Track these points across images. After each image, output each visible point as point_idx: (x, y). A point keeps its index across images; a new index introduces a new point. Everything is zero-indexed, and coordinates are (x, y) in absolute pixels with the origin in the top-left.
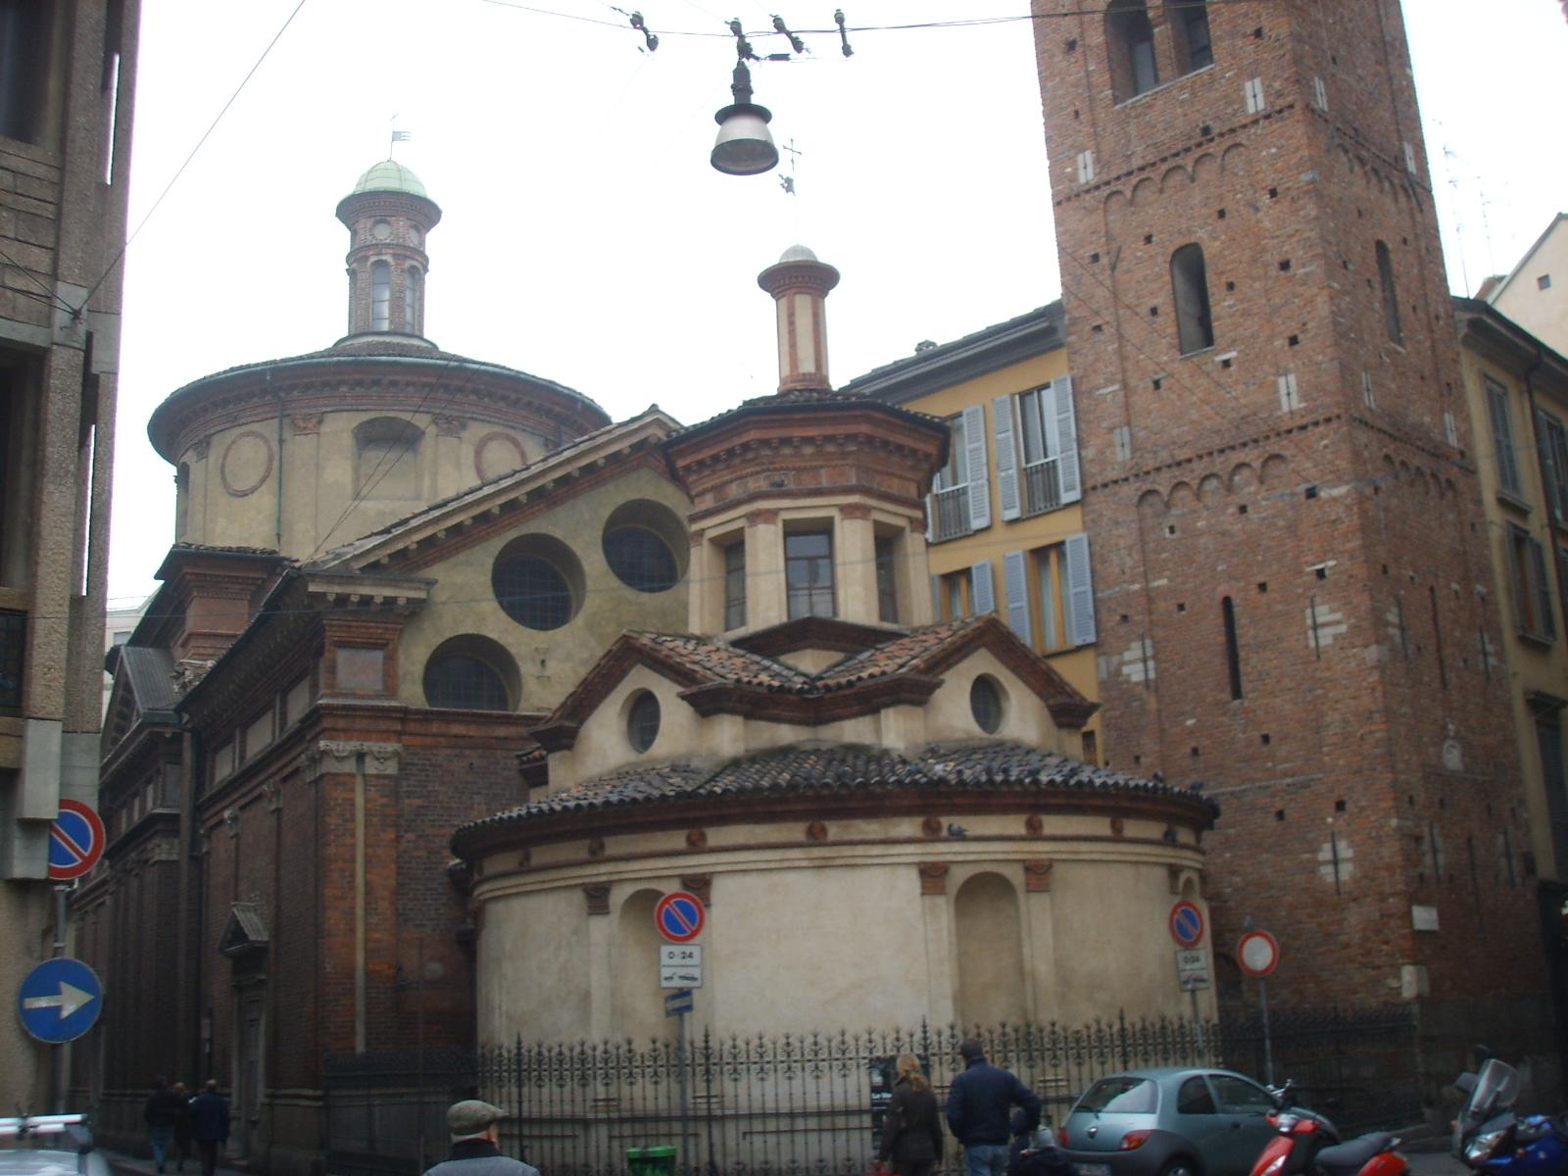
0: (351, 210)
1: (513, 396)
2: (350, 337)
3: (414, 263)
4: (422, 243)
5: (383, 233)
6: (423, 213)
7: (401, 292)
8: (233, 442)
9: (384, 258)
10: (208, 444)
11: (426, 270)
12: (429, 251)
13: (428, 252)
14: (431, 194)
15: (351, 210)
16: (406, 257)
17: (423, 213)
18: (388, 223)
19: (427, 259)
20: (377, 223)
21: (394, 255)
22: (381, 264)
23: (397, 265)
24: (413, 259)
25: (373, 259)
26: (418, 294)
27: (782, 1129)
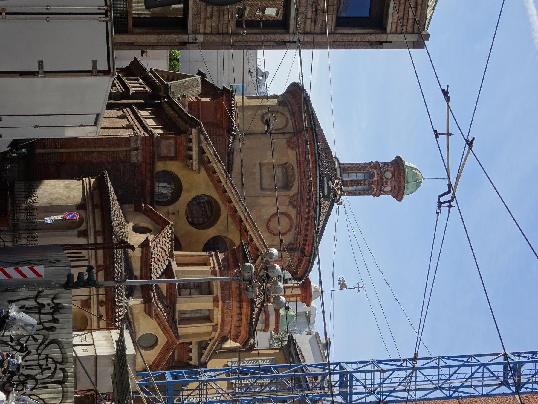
0: (398, 162)
1: (309, 227)
2: (339, 164)
3: (375, 190)
4: (385, 193)
5: (388, 175)
6: (398, 194)
7: (361, 184)
8: (284, 115)
9: (376, 176)
10: (284, 106)
11: (374, 195)
12: (383, 198)
13: (381, 196)
14: (406, 197)
15: (398, 162)
16: (378, 185)
17: (398, 194)
18: (392, 177)
19: (378, 196)
20: (392, 173)
21: (377, 180)
22: (373, 176)
23: (373, 182)
24: (377, 188)
25: (375, 171)
26: (362, 192)
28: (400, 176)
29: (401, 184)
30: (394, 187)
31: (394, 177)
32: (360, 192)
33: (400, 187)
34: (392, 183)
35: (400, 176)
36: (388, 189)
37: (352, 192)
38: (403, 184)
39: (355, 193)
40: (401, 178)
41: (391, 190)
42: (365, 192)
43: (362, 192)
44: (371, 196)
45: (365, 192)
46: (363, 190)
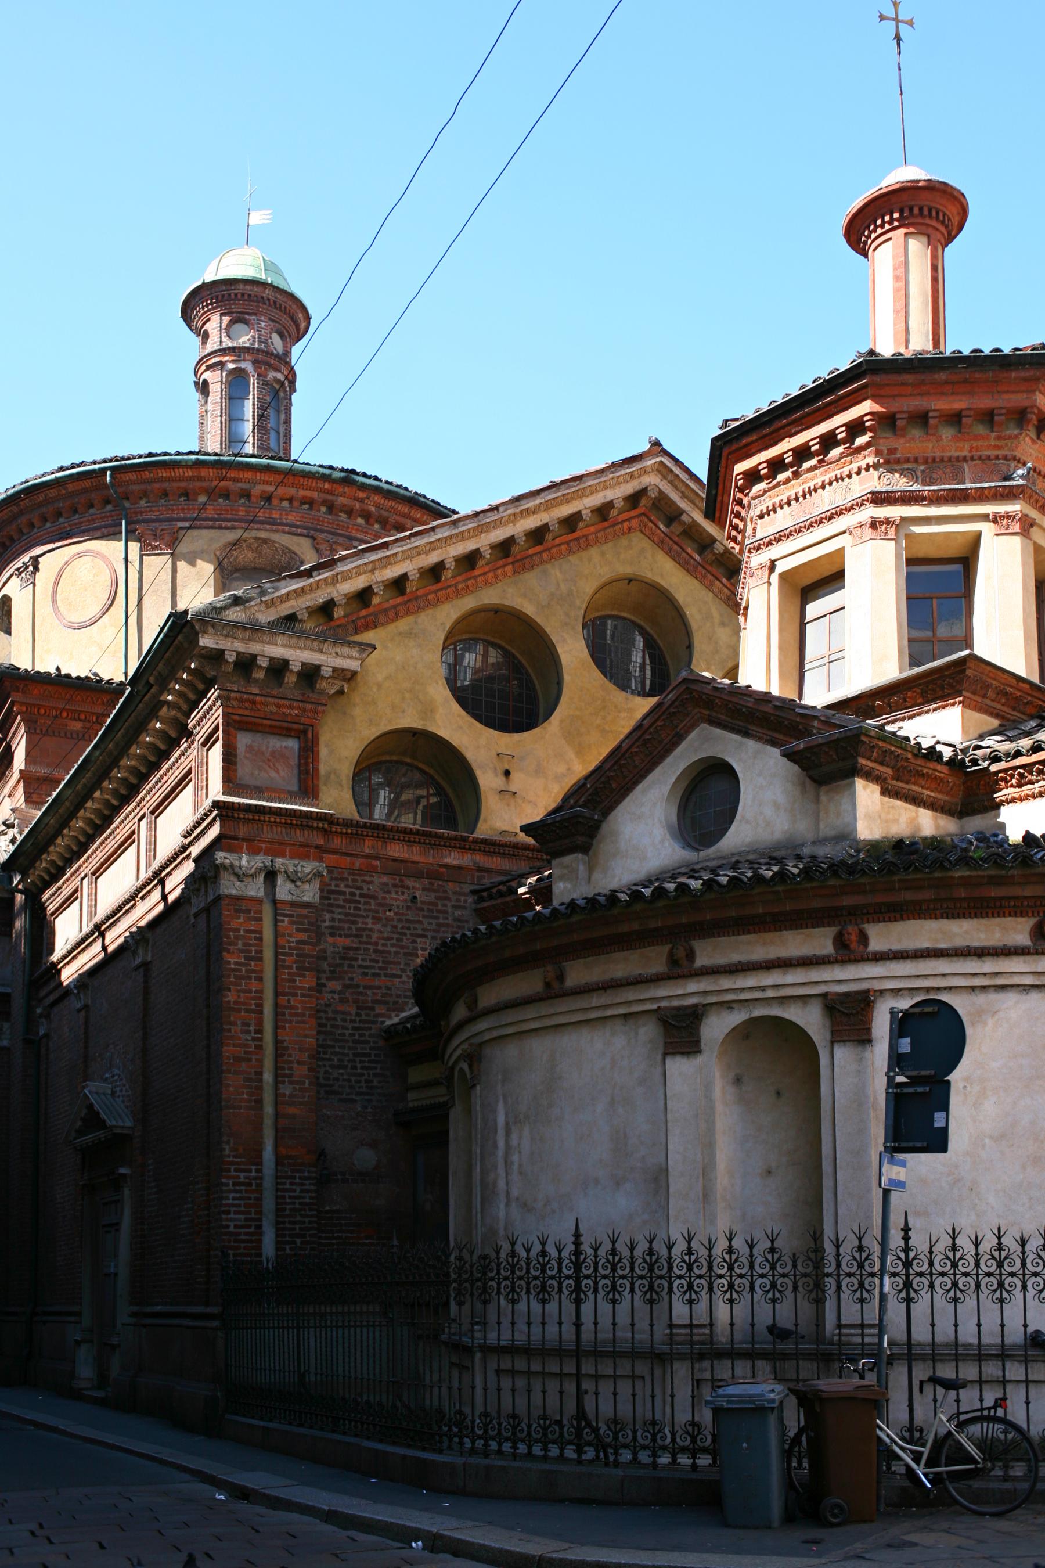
4: (287, 353)
9: (243, 365)
11: (293, 389)
18: (246, 322)
21: (256, 363)
24: (277, 370)
25: (231, 366)
27: (574, 1371)
28: (246, 297)
29: (269, 299)
30: (273, 321)
31: (247, 317)
32: (282, 422)
33: (275, 302)
34: (263, 324)
35: (246, 297)
36: (277, 343)
37: (281, 442)
38: (267, 291)
39: (285, 436)
40: (249, 295)
41: (281, 335)
42: (283, 408)
43: (283, 417)
44: (294, 397)
45: (283, 408)
46: (278, 411)
